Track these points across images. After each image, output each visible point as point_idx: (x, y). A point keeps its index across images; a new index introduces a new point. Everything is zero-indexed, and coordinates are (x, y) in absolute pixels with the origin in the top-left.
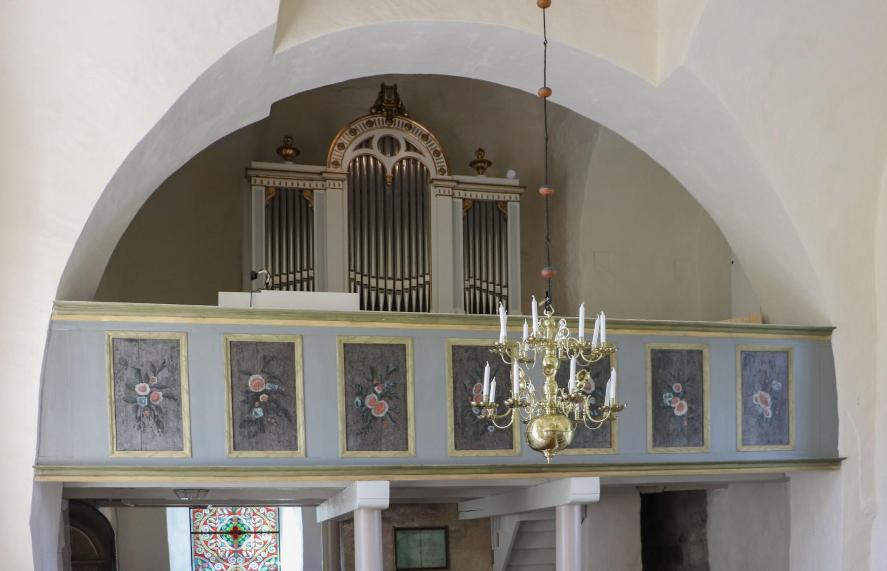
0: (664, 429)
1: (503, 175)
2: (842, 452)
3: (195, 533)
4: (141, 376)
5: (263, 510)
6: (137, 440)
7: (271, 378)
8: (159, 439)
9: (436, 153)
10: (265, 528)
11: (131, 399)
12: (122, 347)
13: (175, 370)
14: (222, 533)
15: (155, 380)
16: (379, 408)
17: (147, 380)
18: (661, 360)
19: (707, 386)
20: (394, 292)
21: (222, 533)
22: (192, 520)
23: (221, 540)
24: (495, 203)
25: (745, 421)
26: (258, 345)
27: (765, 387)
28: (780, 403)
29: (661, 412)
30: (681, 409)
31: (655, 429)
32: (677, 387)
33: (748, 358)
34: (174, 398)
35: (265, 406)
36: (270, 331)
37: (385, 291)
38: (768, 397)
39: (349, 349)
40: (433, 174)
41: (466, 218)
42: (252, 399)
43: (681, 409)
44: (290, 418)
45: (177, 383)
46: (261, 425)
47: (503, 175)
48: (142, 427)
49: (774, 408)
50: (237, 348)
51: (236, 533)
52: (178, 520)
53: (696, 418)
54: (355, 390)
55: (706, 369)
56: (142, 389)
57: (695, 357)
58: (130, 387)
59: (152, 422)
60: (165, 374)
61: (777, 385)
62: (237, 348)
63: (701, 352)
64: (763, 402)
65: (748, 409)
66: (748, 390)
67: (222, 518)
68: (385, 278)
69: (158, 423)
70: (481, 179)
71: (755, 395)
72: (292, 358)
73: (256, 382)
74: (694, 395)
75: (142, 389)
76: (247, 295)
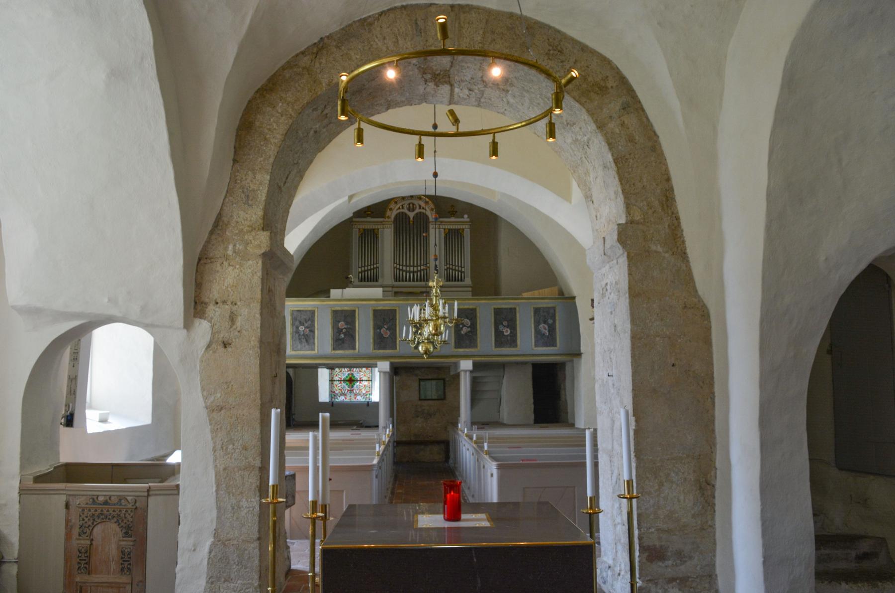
0: (500, 340)
1: (463, 217)
2: (583, 349)
3: (332, 381)
4: (301, 324)
5: (364, 369)
6: (299, 347)
7: (347, 323)
8: (307, 347)
9: (432, 209)
10: (365, 378)
11: (297, 332)
12: (295, 313)
13: (313, 321)
14: (344, 381)
15: (306, 325)
16: (386, 333)
17: (303, 325)
18: (498, 312)
19: (518, 322)
20: (413, 272)
21: (344, 381)
22: (331, 374)
23: (343, 384)
24: (458, 230)
25: (536, 337)
26: (342, 311)
27: (545, 322)
28: (552, 329)
29: (498, 334)
30: (507, 332)
31: (496, 341)
32: (505, 323)
33: (537, 311)
34: (313, 331)
35: (344, 333)
36: (346, 306)
37: (410, 272)
38: (546, 326)
39: (375, 312)
40: (431, 219)
41: (445, 238)
42: (340, 331)
43: (507, 332)
44: (353, 338)
45: (314, 326)
46: (343, 341)
47: (463, 217)
48: (301, 342)
49: (549, 331)
50: (335, 313)
51: (351, 381)
52: (323, 375)
53: (514, 335)
54: (377, 327)
55: (518, 315)
56: (302, 328)
57: (513, 311)
58: (297, 328)
59: (304, 340)
60: (309, 322)
61: (550, 321)
62: (335, 313)
63: (515, 309)
64: (544, 328)
65: (538, 332)
66: (537, 324)
67: (344, 373)
68: (410, 266)
69: (307, 341)
70: (453, 219)
71: (541, 326)
72: (354, 316)
73: (342, 325)
74: (512, 326)
75: (302, 328)
76: (340, 290)
